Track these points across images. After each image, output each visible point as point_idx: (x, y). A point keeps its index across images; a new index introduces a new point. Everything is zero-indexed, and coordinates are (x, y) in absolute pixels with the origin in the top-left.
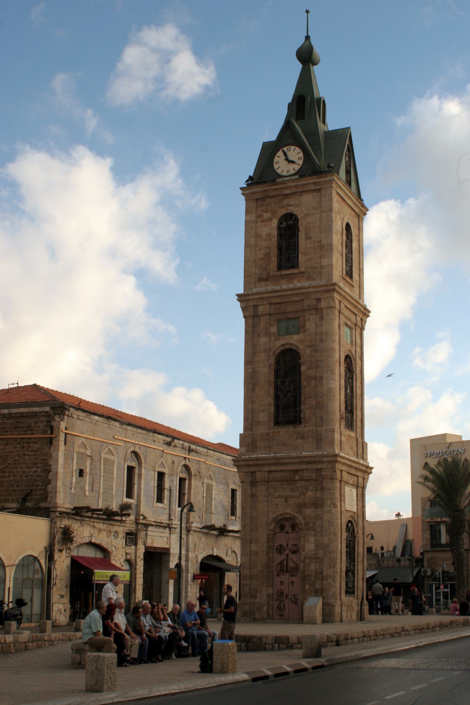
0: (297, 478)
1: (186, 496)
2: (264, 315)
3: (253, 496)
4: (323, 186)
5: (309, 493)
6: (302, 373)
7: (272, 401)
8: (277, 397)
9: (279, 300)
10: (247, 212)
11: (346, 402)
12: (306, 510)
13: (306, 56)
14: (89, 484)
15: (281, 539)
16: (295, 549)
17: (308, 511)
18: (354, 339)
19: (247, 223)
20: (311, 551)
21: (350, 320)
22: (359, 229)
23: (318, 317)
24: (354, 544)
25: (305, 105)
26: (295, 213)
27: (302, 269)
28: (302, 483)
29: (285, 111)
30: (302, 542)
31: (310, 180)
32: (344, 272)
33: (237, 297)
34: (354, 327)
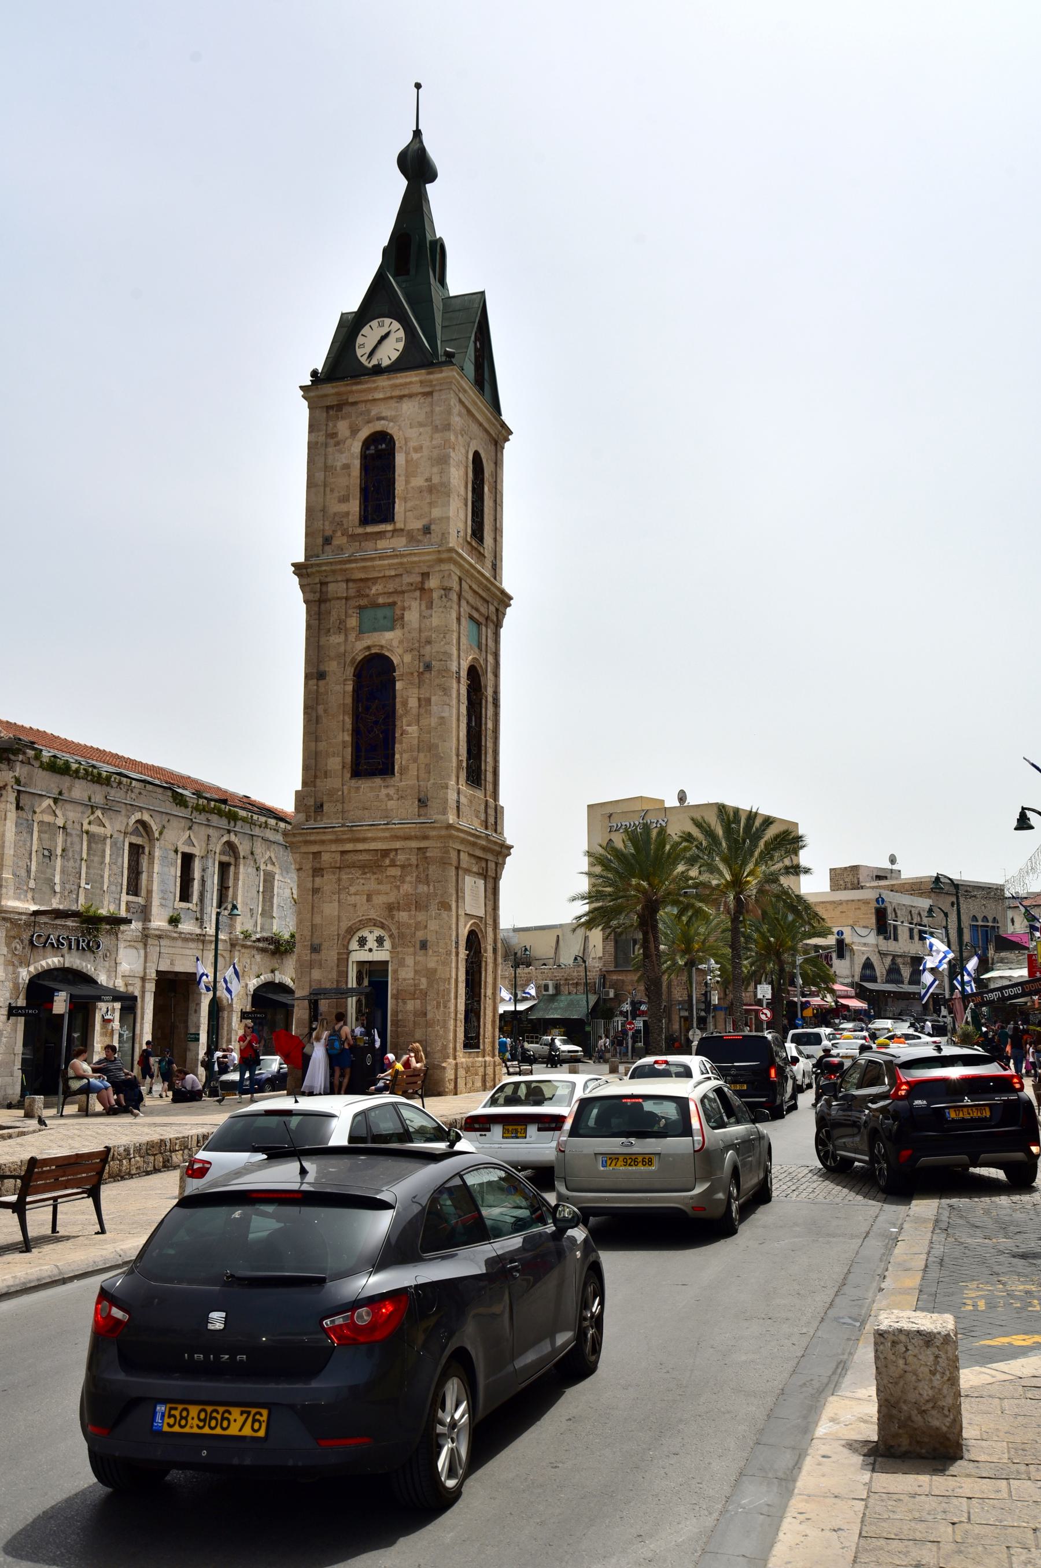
1: (231, 890)
2: (338, 598)
3: (315, 891)
5: (406, 888)
6: (398, 694)
7: (348, 738)
8: (356, 732)
9: (363, 576)
10: (312, 427)
11: (469, 742)
12: (401, 913)
13: (416, 166)
14: (63, 872)
17: (403, 916)
18: (484, 641)
19: (312, 446)
21: (477, 610)
22: (496, 463)
23: (424, 604)
24: (480, 968)
25: (413, 251)
26: (389, 431)
27: (399, 525)
28: (395, 872)
29: (377, 261)
31: (413, 378)
32: (469, 531)
33: (293, 569)
34: (484, 622)
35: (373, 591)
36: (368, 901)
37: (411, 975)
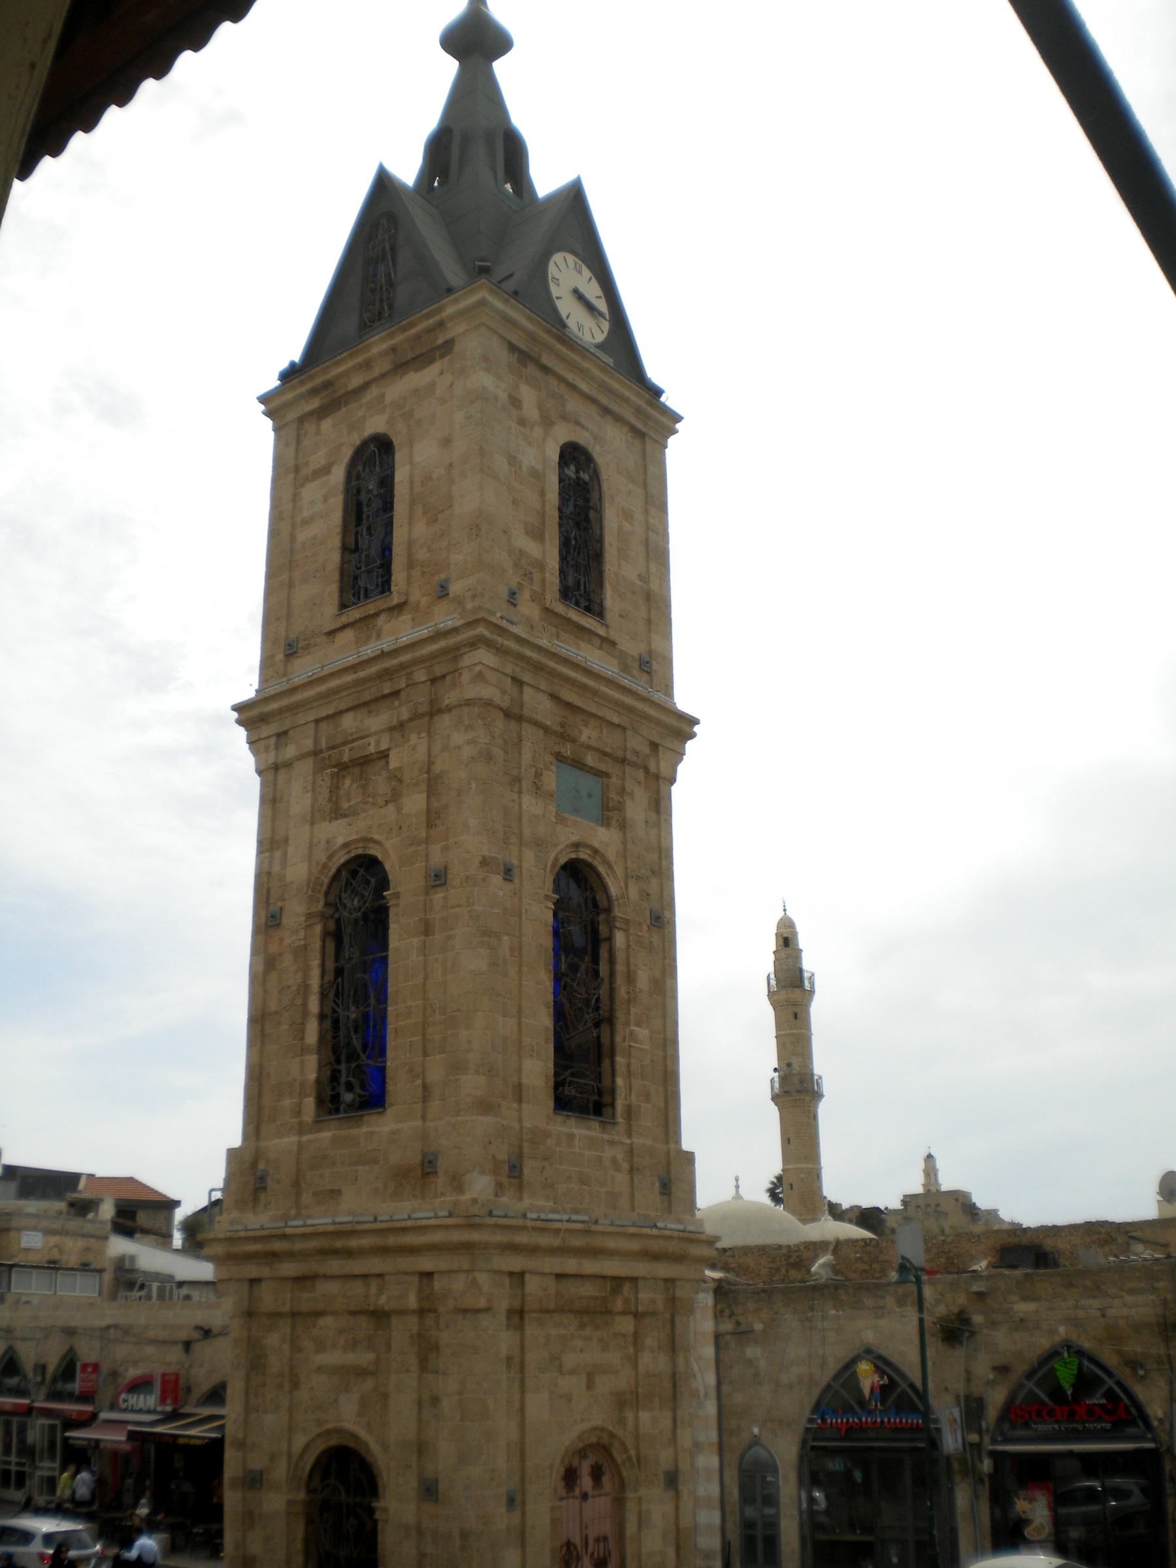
4: (651, 433)
8: (559, 1015)
27: (614, 635)
28: (626, 1325)
30: (631, 1528)
35: (584, 738)
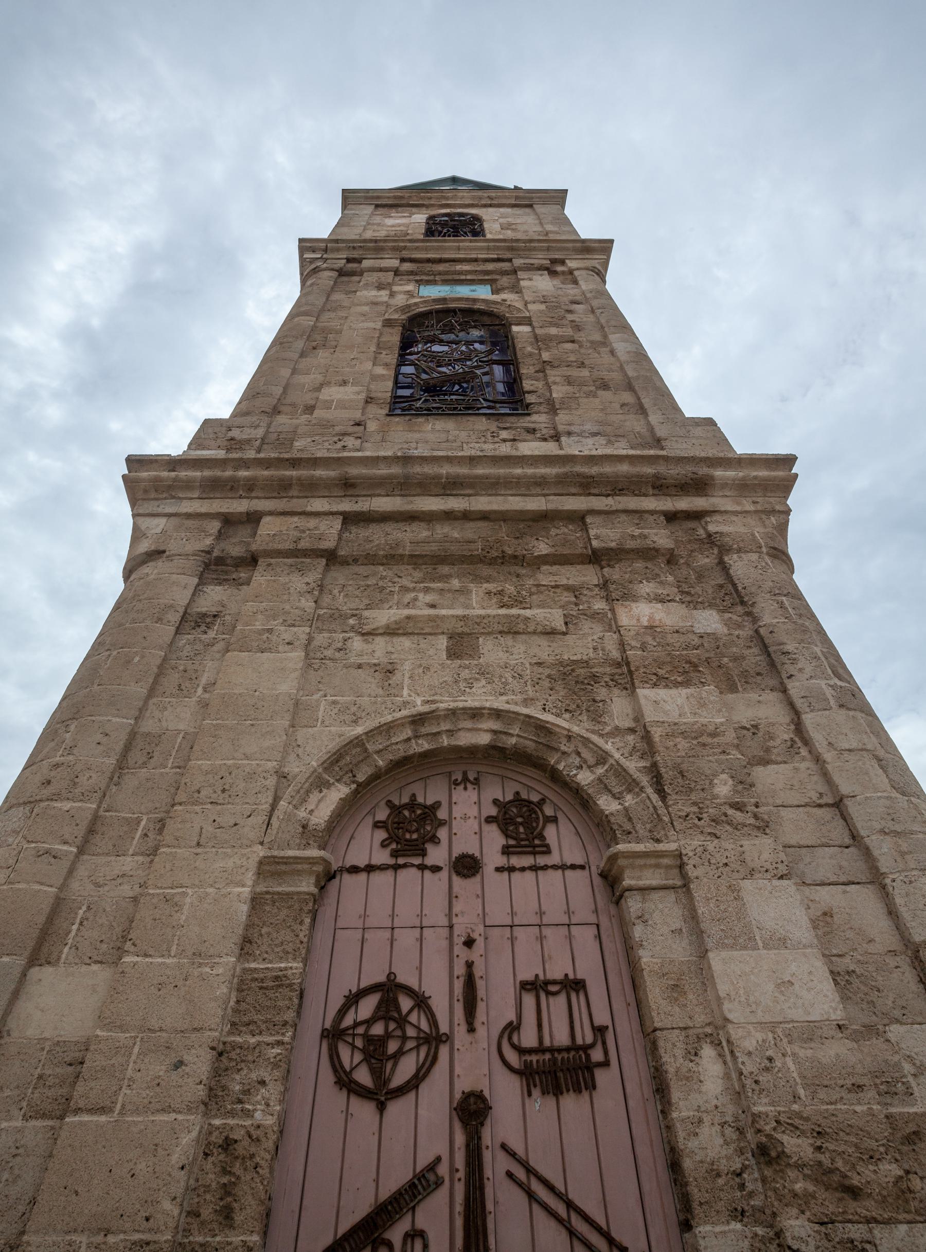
0: (542, 548)
15: (398, 925)
16: (562, 1038)
20: (810, 1033)
36: (452, 654)
37: (819, 1000)
